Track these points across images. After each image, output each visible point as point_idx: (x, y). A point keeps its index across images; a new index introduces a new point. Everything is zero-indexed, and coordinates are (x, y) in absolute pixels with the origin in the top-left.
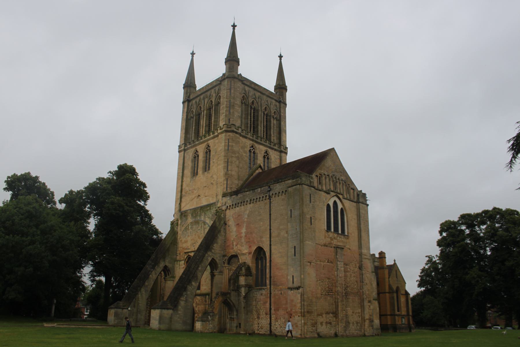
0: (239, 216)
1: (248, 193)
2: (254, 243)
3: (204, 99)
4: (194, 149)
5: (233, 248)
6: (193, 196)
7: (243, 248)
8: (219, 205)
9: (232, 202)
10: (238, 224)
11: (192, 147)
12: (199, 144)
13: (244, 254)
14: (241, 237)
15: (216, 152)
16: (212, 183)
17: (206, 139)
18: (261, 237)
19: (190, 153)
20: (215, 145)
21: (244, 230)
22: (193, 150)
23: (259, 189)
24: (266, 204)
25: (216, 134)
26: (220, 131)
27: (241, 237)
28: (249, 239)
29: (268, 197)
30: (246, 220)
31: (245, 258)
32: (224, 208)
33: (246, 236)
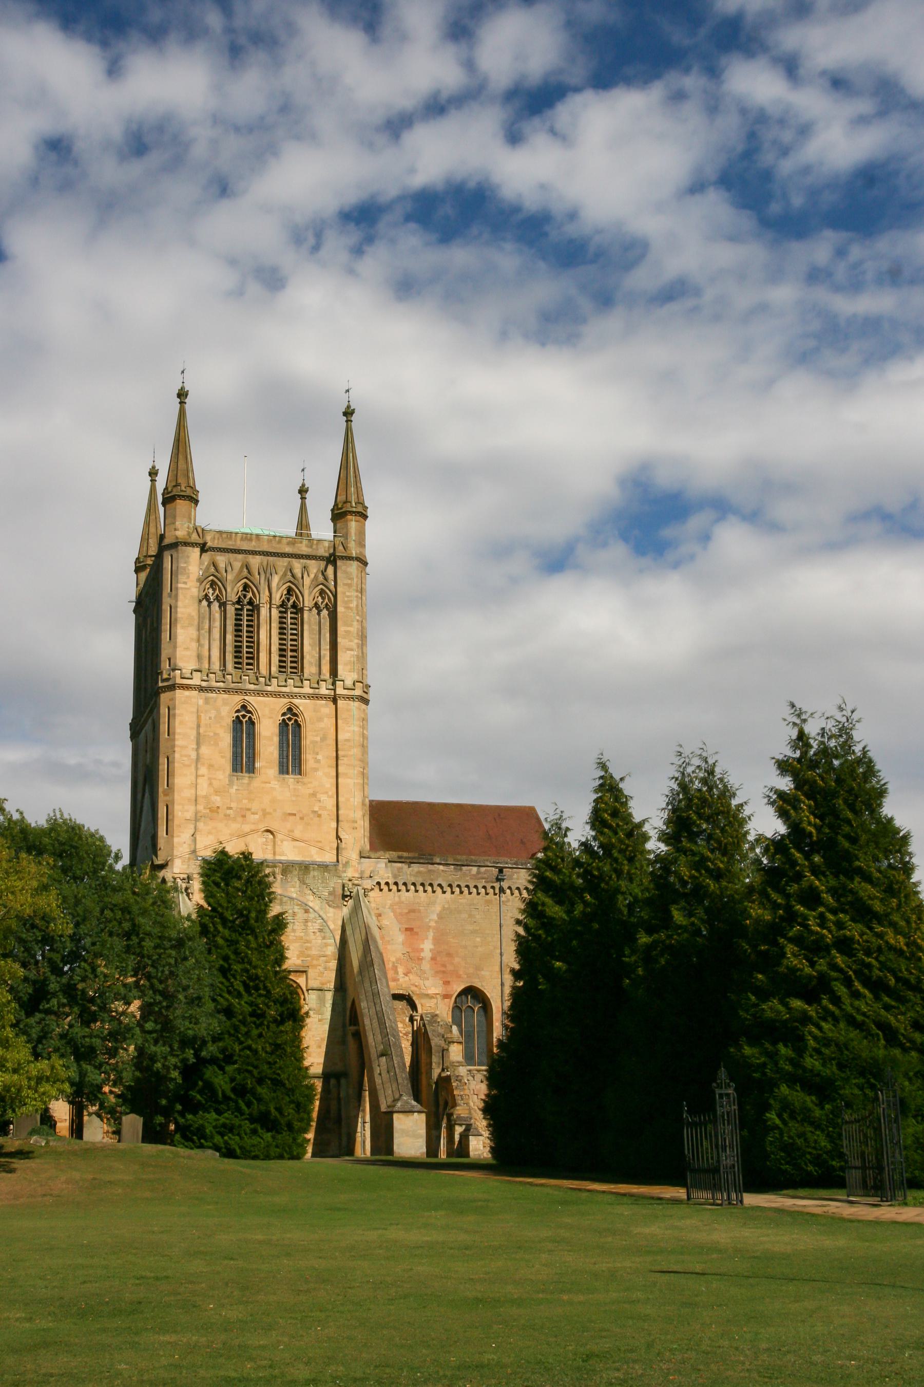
0: (413, 911)
1: (441, 867)
2: (459, 976)
3: (268, 572)
4: (237, 699)
5: (395, 980)
6: (247, 828)
7: (427, 983)
8: (350, 873)
9: (395, 876)
10: (409, 929)
11: (226, 691)
12: (259, 693)
13: (428, 996)
14: (420, 959)
15: (324, 739)
16: (315, 812)
17: (284, 689)
18: (478, 968)
19: (225, 707)
20: (320, 719)
21: (427, 946)
22: (237, 699)
23: (475, 869)
24: (488, 902)
25: (323, 691)
26: (346, 692)
27: (420, 959)
28: (444, 966)
29: (497, 891)
30: (433, 924)
31: (432, 1005)
32: (368, 884)
33: (433, 959)
